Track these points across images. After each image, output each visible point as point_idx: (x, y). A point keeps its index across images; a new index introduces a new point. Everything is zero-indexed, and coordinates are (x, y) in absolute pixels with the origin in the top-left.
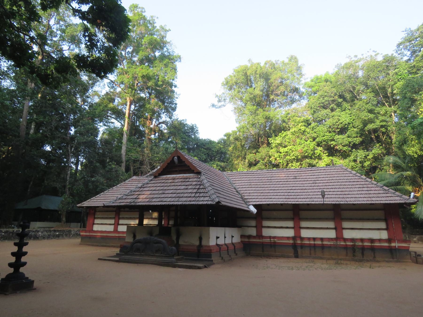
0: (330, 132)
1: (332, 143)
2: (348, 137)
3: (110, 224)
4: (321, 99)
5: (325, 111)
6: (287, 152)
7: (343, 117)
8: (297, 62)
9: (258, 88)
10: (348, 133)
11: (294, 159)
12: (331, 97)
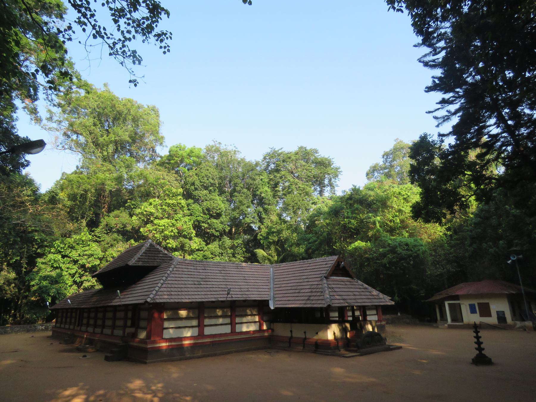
0: (205, 214)
1: (204, 225)
2: (222, 223)
3: (192, 327)
4: (206, 178)
5: (205, 191)
6: (164, 226)
7: (219, 202)
8: (158, 116)
9: (123, 132)
10: (221, 219)
11: (171, 236)
12: (213, 179)
